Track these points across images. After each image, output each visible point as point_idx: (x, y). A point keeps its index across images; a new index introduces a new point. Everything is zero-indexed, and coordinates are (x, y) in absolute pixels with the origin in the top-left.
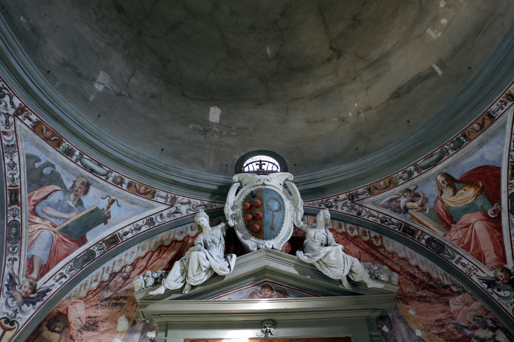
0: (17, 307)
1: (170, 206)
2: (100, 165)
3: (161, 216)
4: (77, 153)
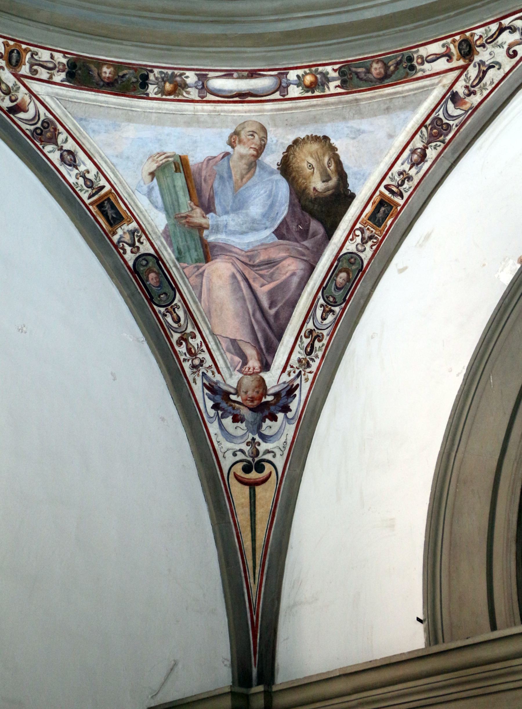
0: (250, 434)
1: (461, 70)
2: (253, 74)
3: (455, 98)
4: (191, 78)
